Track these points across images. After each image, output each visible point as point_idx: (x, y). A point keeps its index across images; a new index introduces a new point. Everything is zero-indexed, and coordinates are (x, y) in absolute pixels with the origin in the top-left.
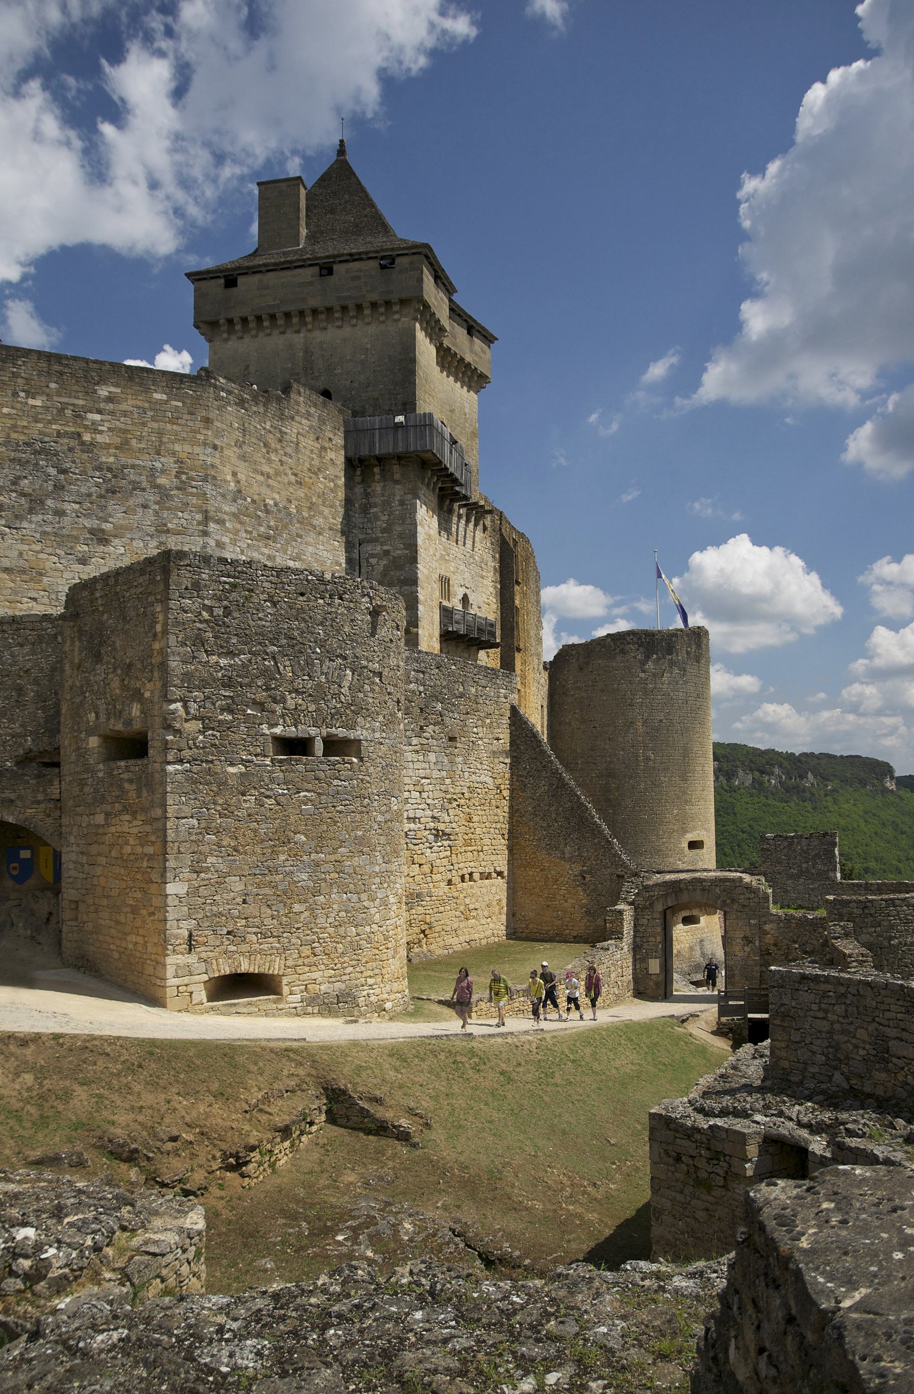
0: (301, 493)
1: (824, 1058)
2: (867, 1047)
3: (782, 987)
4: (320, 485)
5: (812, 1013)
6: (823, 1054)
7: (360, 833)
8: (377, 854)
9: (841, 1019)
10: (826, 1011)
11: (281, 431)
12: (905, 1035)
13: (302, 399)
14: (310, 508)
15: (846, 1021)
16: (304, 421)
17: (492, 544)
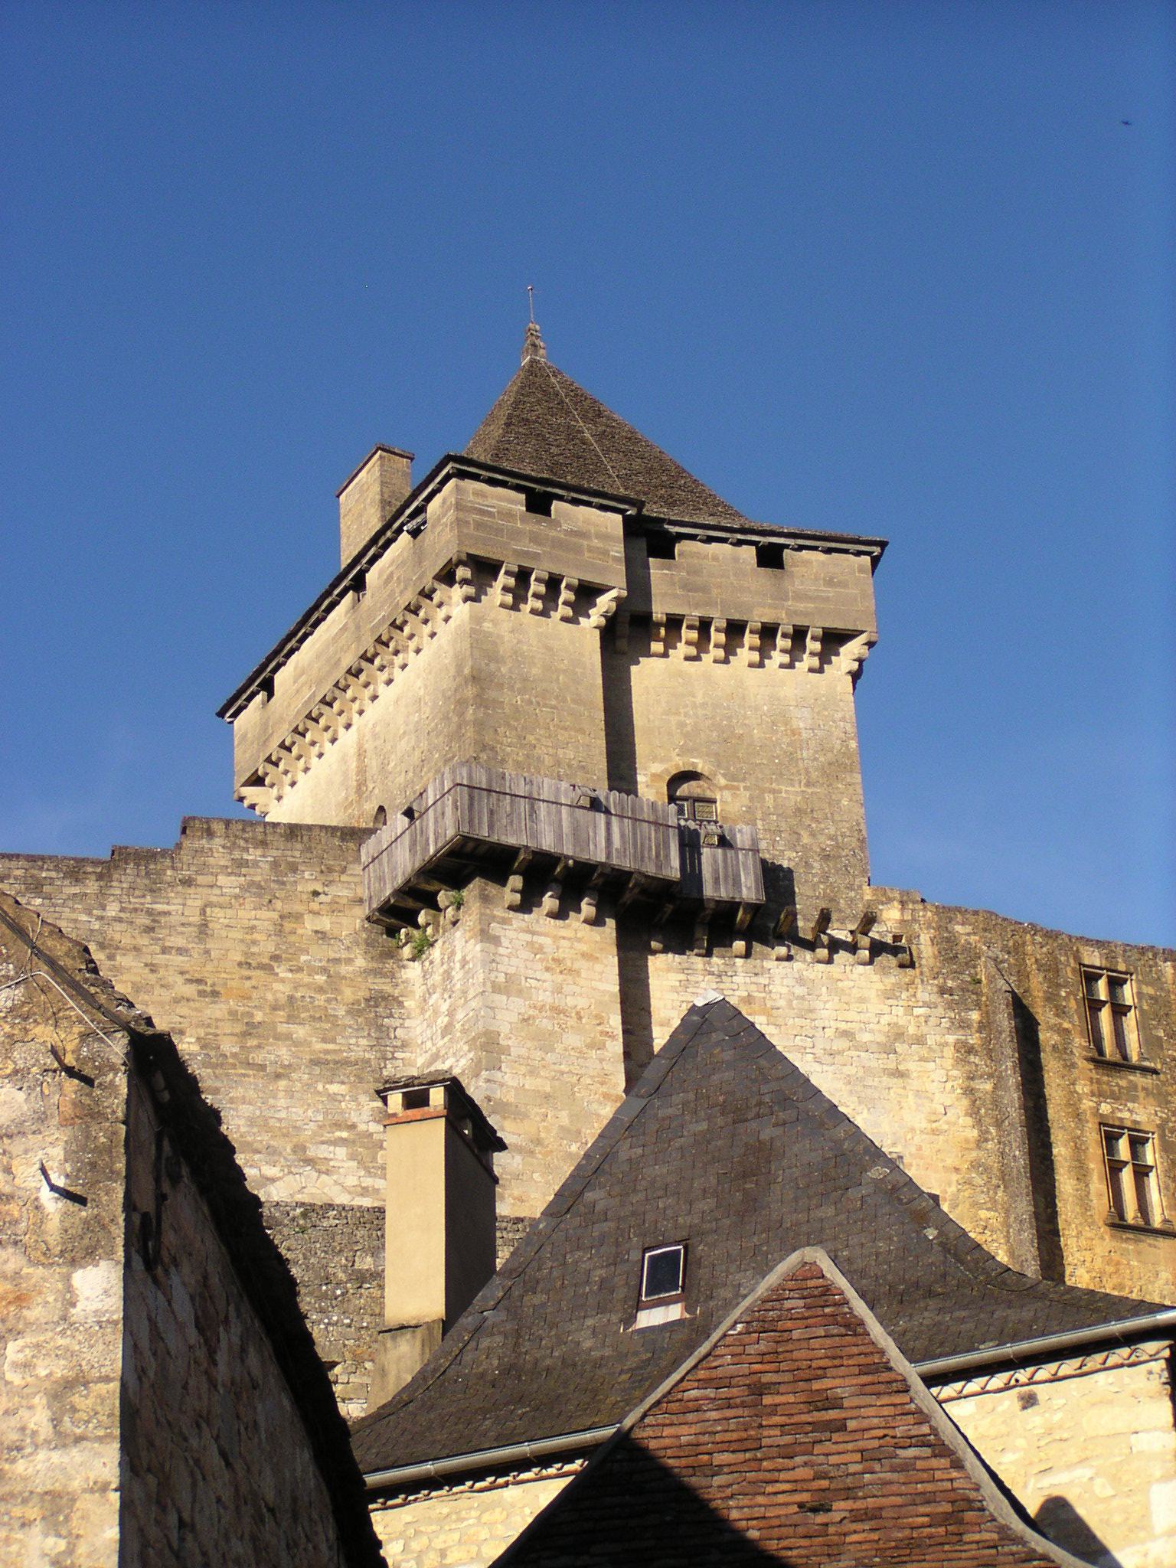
0: (217, 1010)
4: (277, 986)
11: (149, 913)
13: (217, 841)
14: (245, 1034)
16: (222, 880)
17: (942, 991)
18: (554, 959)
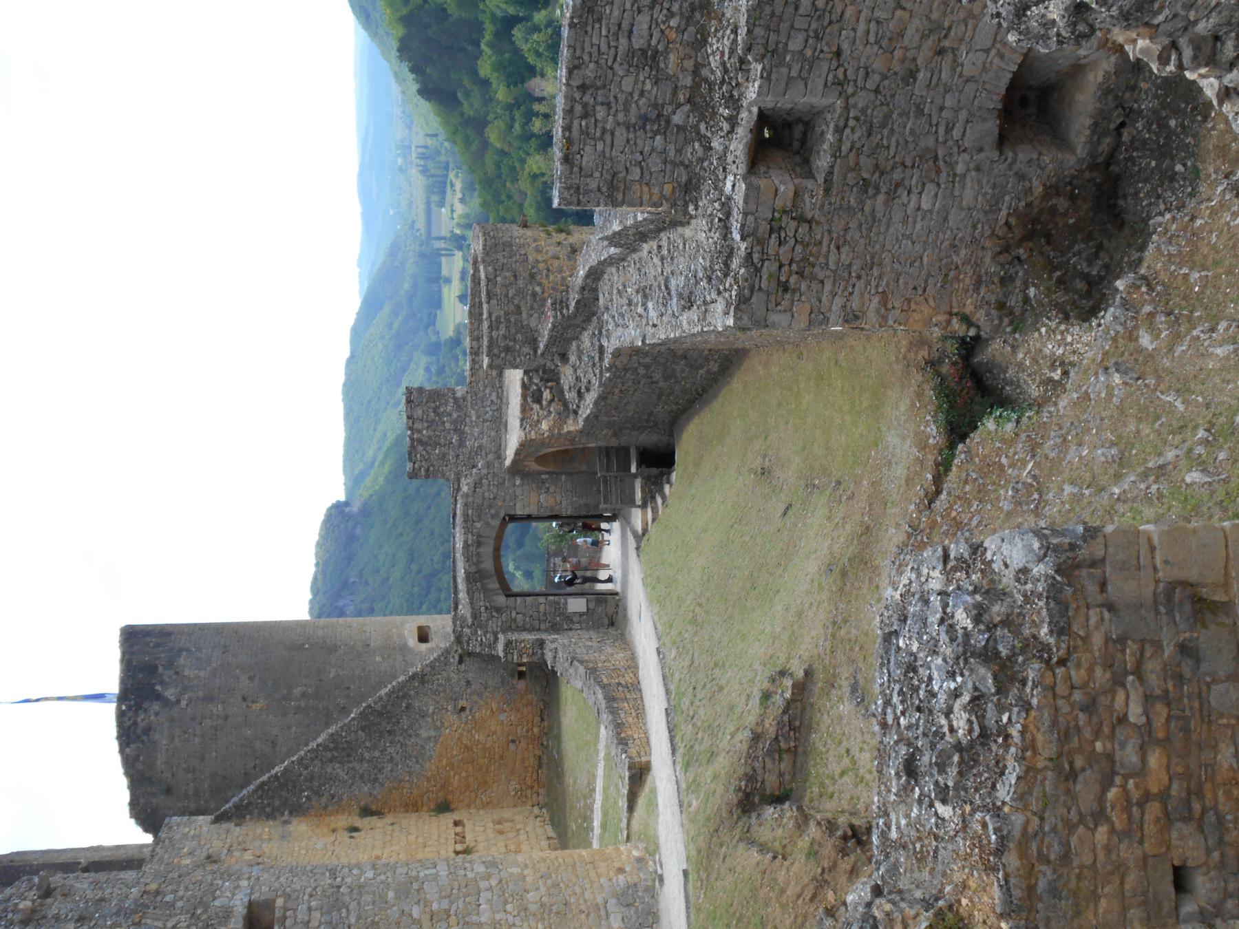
1: (658, 137)
2: (642, 78)
3: (578, 188)
5: (607, 150)
6: (653, 138)
7: (391, 894)
8: (422, 874)
9: (612, 111)
10: (604, 131)
12: (625, 25)
15: (613, 105)
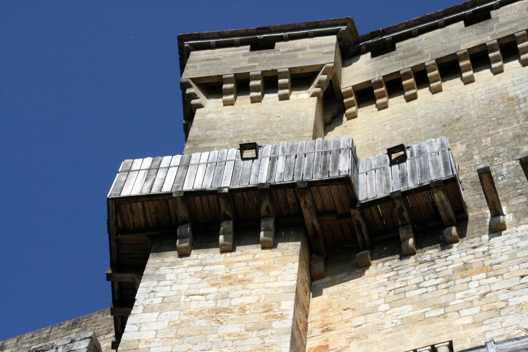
18: (223, 277)
